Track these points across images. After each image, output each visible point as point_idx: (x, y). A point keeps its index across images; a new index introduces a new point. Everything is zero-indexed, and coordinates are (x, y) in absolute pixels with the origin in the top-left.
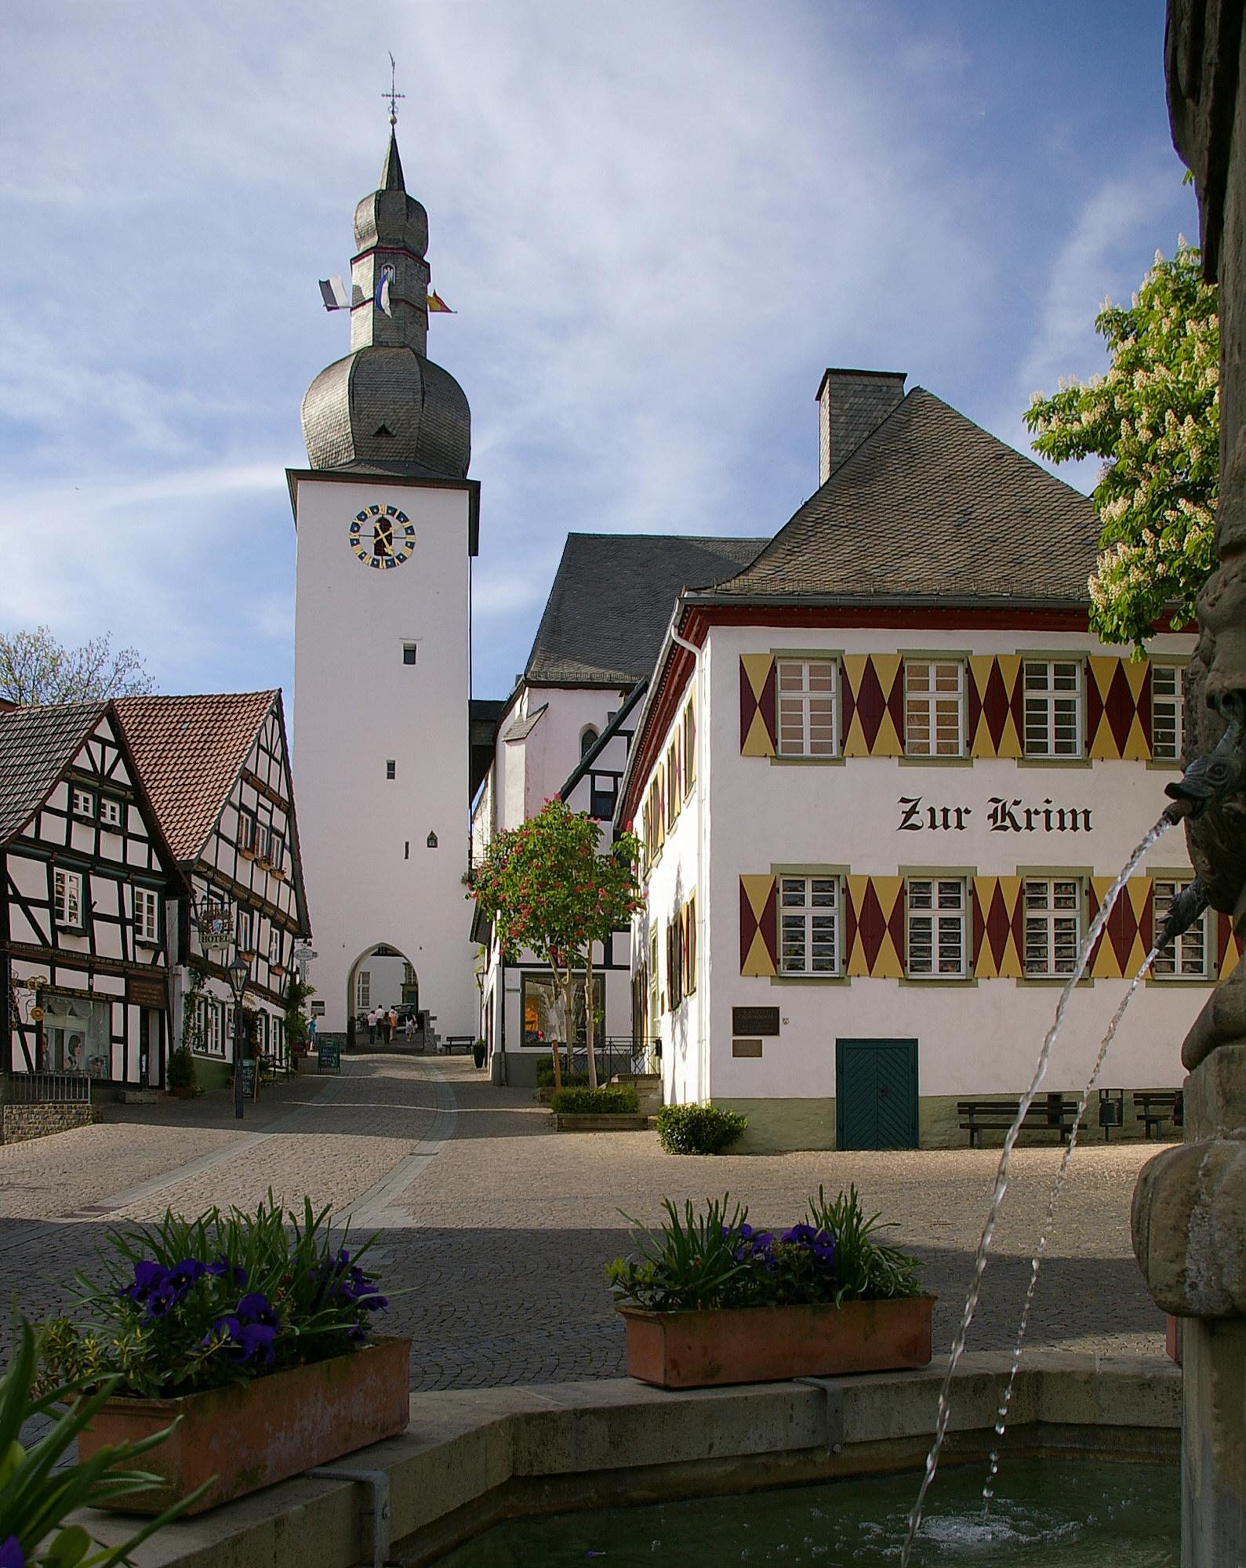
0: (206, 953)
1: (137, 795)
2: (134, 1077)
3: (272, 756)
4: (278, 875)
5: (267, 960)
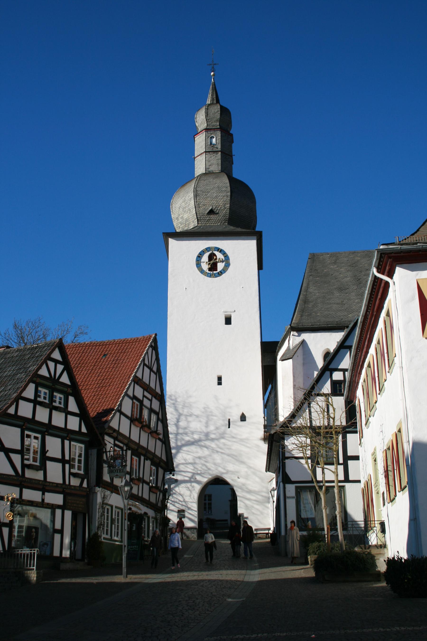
0: (112, 480)
1: (74, 390)
2: (66, 553)
3: (151, 370)
4: (154, 435)
5: (148, 484)
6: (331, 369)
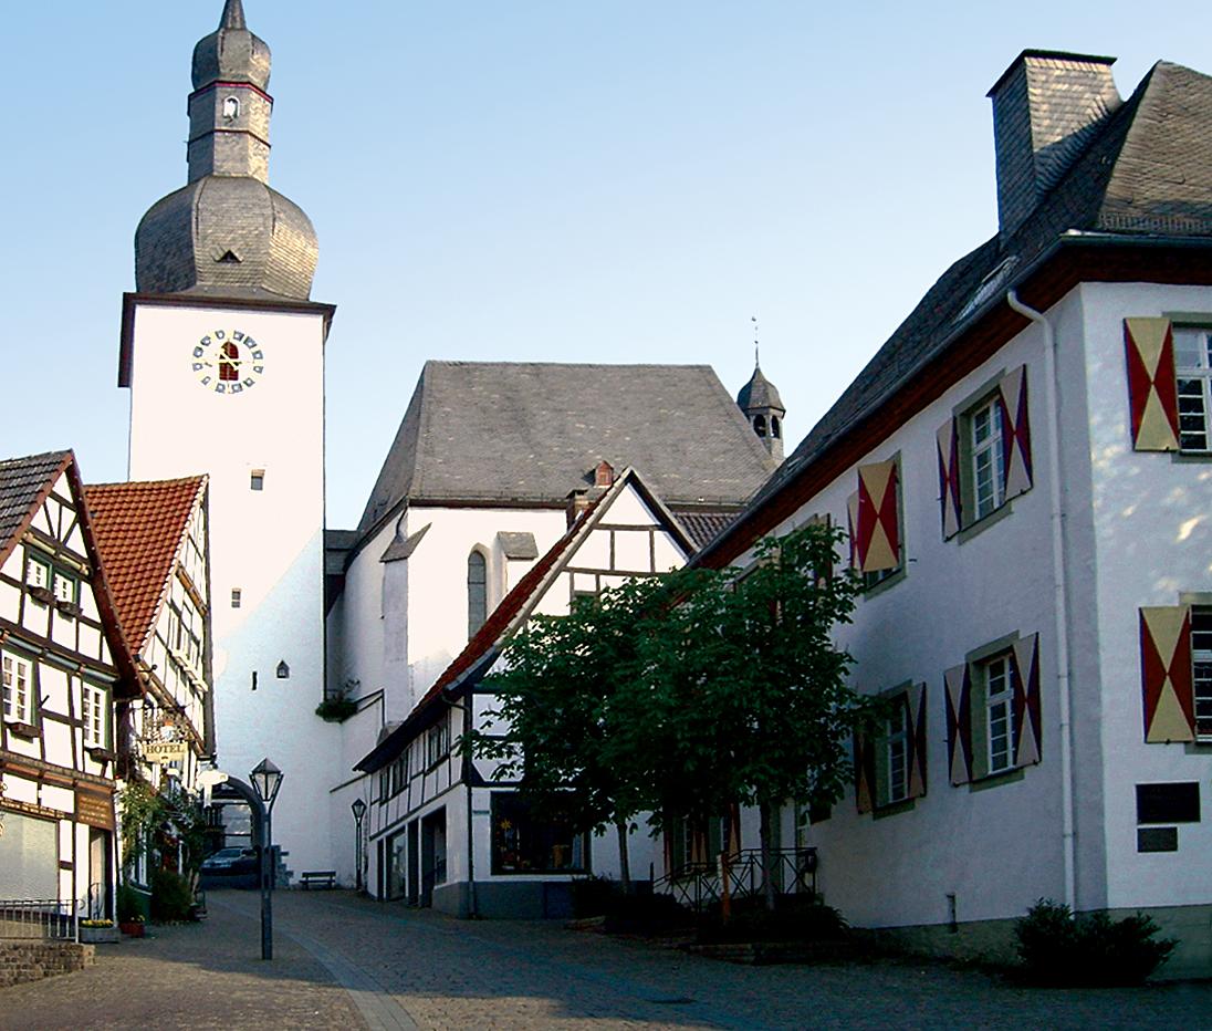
6: (572, 569)
